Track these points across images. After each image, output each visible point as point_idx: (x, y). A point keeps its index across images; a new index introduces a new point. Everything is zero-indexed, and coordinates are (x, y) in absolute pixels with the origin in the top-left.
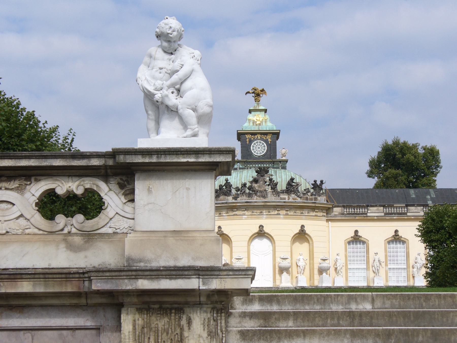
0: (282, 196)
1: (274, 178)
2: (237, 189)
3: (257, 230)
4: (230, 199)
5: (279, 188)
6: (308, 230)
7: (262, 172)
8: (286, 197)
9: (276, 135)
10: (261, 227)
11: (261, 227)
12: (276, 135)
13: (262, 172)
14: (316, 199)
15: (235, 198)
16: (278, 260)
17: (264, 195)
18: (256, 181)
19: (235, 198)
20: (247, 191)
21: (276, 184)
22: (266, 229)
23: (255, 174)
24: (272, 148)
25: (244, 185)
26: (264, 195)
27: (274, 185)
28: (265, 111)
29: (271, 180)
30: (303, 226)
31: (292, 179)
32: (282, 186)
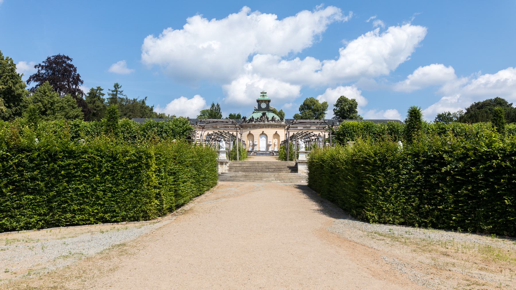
0: (270, 122)
1: (268, 116)
2: (256, 119)
3: (261, 133)
4: (253, 123)
5: (269, 119)
6: (278, 132)
7: (264, 114)
8: (271, 122)
9: (269, 101)
10: (263, 131)
11: (263, 131)
12: (269, 101)
13: (264, 114)
14: (281, 123)
15: (255, 122)
16: (268, 142)
17: (264, 122)
18: (261, 117)
19: (255, 122)
20: (259, 120)
21: (268, 118)
22: (265, 132)
23: (262, 115)
24: (268, 106)
25: (258, 118)
26: (264, 122)
27: (267, 118)
28: (266, 93)
29: (266, 117)
30: (276, 132)
31: (273, 116)
32: (270, 119)
